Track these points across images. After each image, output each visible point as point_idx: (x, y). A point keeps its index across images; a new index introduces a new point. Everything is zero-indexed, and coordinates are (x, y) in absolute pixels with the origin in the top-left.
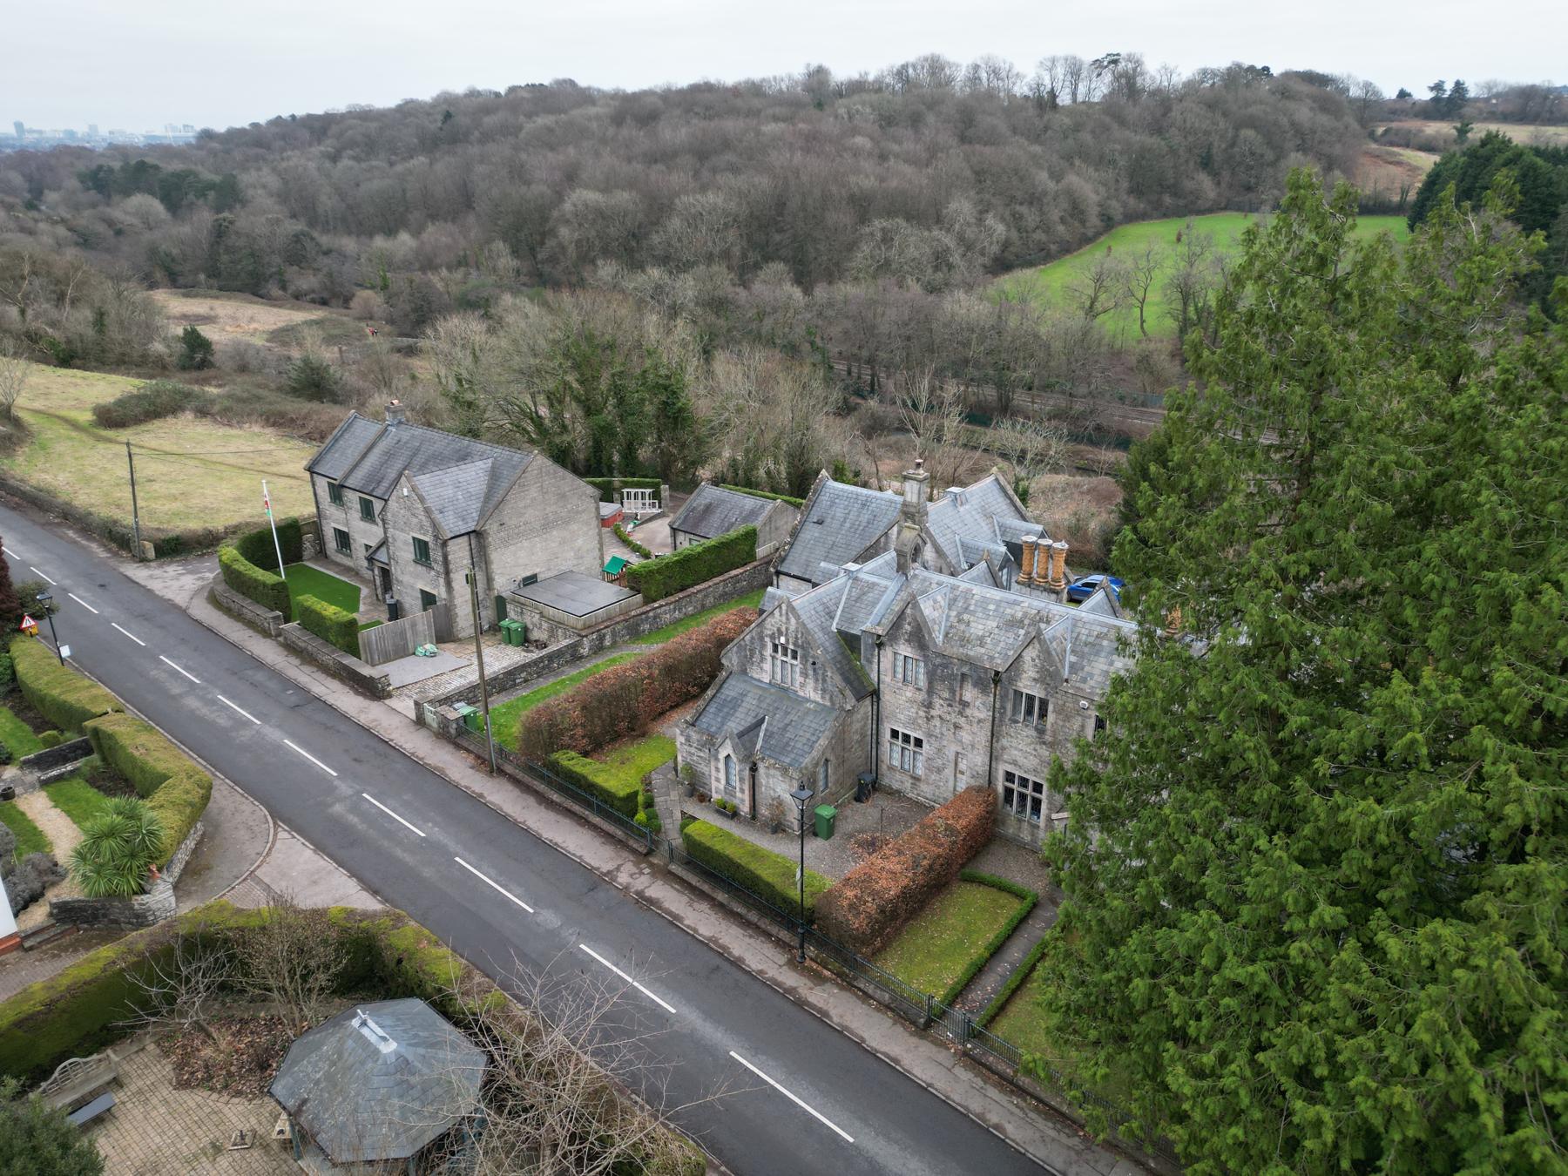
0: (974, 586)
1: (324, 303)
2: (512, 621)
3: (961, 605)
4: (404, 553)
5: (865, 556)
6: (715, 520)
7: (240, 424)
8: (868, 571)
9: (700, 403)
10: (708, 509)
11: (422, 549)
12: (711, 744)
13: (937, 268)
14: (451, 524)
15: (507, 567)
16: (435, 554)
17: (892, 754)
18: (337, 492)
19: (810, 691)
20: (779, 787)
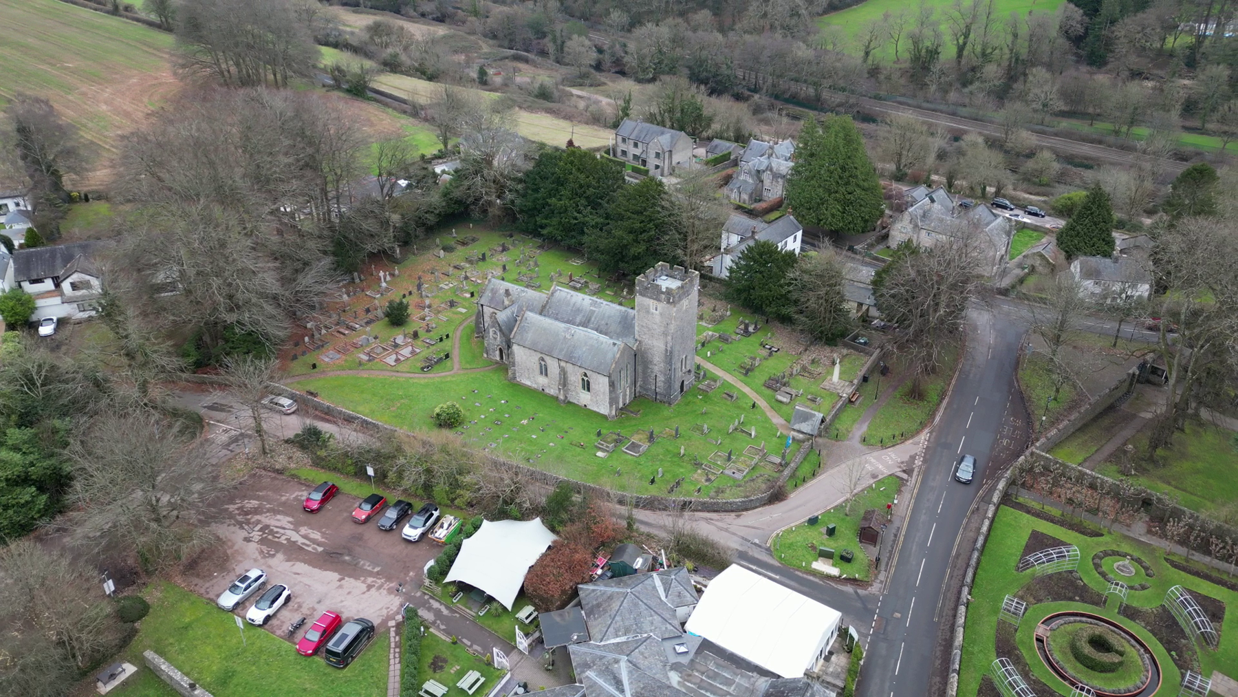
0: (782, 161)
1: (441, 19)
2: (677, 171)
3: (779, 164)
4: (652, 155)
5: (761, 156)
6: (718, 150)
7: (536, 112)
8: (762, 159)
9: (706, 112)
10: (716, 146)
11: (658, 155)
12: (732, 190)
13: (791, 16)
14: (666, 149)
15: (676, 159)
16: (662, 156)
17: (765, 193)
18: (624, 140)
19: (751, 181)
20: (745, 197)
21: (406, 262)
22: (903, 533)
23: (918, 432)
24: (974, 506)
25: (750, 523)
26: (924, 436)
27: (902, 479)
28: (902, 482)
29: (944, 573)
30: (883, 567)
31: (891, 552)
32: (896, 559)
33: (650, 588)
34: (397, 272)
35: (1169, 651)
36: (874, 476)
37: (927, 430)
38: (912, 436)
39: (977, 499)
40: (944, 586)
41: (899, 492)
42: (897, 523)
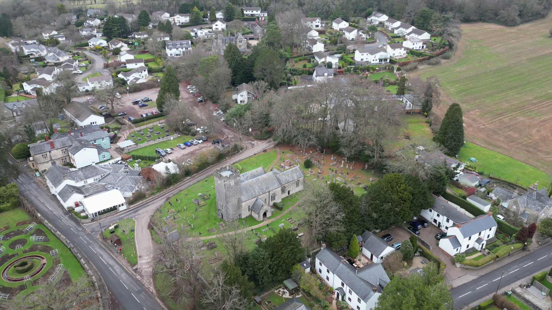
21: (363, 172)
22: (111, 254)
23: (155, 287)
24: (103, 280)
25: (145, 218)
26: (152, 289)
27: (133, 266)
28: (133, 265)
29: (86, 254)
30: (103, 241)
31: (107, 246)
32: (102, 245)
33: (128, 182)
34: (351, 168)
35: (4, 287)
36: (140, 257)
37: (154, 292)
38: (154, 284)
39: (105, 284)
40: (83, 252)
41: (129, 262)
42: (116, 254)
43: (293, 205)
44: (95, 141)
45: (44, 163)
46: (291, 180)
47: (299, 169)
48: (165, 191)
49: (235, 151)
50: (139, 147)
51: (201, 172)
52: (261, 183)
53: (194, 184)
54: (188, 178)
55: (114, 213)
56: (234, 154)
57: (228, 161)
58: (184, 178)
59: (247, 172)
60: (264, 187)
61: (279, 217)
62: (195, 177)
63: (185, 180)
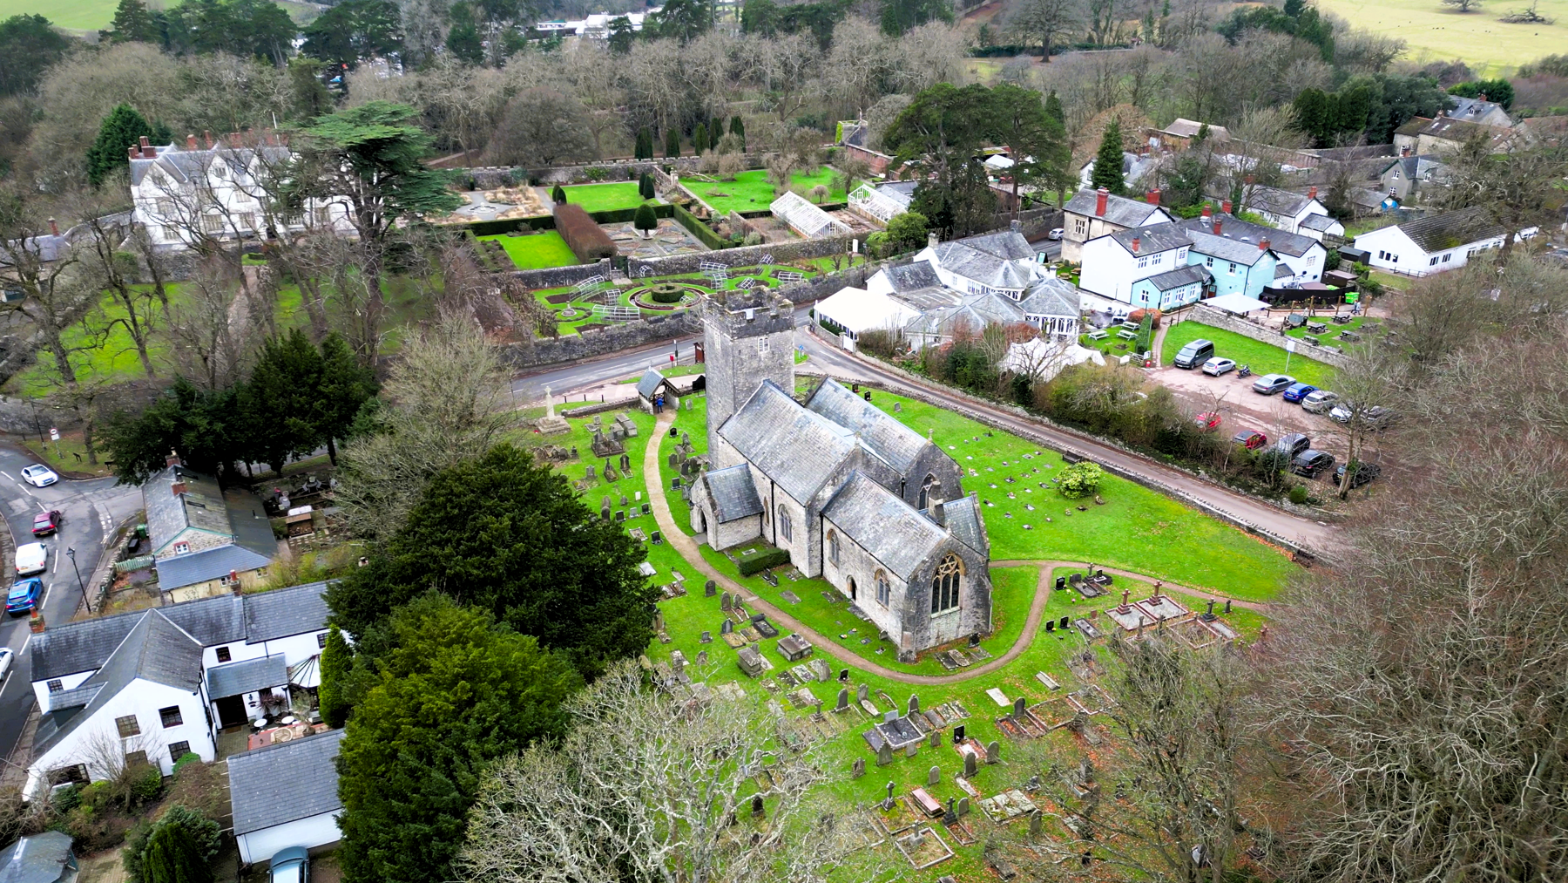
43: (778, 608)
44: (1211, 258)
45: (1074, 242)
46: (862, 538)
47: (932, 544)
48: (936, 385)
49: (1260, 476)
50: (1232, 328)
51: (1070, 429)
52: (796, 440)
53: (969, 417)
54: (1019, 410)
55: (831, 341)
56: (1248, 488)
57: (1188, 482)
58: (1008, 400)
59: (883, 414)
60: (784, 457)
61: (704, 568)
62: (1038, 426)
63: (1005, 406)
